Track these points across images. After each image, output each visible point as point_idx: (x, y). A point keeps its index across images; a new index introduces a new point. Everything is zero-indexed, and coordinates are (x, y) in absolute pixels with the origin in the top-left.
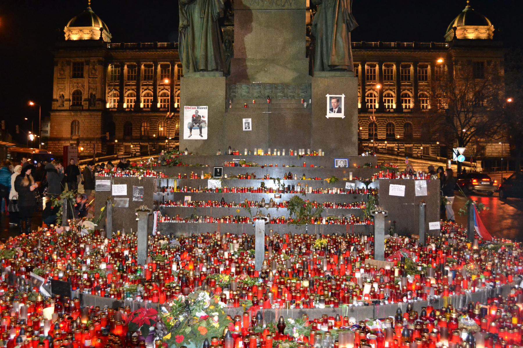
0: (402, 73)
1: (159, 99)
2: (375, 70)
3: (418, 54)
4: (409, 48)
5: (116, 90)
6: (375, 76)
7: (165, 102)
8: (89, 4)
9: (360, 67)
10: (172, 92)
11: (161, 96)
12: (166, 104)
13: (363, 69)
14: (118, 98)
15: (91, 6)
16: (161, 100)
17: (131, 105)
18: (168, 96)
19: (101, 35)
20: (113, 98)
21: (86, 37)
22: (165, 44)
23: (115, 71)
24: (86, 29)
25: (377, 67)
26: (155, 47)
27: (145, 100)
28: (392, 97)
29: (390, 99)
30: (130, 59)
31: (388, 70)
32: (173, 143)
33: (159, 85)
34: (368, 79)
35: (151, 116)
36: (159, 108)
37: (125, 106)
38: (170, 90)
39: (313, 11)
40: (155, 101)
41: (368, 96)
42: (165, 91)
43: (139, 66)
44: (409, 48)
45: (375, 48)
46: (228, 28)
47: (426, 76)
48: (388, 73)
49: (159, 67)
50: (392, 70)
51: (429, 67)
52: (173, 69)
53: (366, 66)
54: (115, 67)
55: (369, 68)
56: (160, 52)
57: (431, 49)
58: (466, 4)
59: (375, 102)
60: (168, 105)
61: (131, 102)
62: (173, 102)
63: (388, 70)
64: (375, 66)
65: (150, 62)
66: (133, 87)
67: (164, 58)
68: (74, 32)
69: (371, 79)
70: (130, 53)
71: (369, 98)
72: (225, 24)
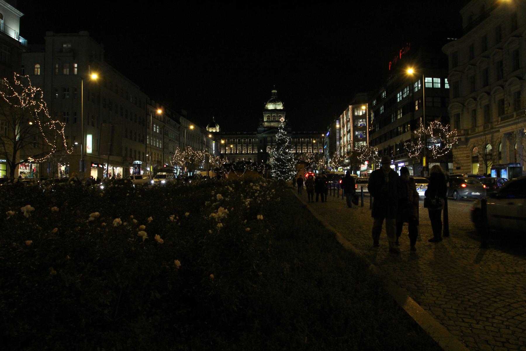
5: (223, 147)
6: (305, 142)
9: (301, 140)
11: (238, 149)
13: (302, 140)
18: (240, 149)
20: (223, 150)
21: (214, 131)
22: (239, 133)
24: (214, 129)
40: (237, 151)
46: (260, 129)
47: (322, 142)
49: (237, 140)
62: (242, 151)
68: (210, 129)
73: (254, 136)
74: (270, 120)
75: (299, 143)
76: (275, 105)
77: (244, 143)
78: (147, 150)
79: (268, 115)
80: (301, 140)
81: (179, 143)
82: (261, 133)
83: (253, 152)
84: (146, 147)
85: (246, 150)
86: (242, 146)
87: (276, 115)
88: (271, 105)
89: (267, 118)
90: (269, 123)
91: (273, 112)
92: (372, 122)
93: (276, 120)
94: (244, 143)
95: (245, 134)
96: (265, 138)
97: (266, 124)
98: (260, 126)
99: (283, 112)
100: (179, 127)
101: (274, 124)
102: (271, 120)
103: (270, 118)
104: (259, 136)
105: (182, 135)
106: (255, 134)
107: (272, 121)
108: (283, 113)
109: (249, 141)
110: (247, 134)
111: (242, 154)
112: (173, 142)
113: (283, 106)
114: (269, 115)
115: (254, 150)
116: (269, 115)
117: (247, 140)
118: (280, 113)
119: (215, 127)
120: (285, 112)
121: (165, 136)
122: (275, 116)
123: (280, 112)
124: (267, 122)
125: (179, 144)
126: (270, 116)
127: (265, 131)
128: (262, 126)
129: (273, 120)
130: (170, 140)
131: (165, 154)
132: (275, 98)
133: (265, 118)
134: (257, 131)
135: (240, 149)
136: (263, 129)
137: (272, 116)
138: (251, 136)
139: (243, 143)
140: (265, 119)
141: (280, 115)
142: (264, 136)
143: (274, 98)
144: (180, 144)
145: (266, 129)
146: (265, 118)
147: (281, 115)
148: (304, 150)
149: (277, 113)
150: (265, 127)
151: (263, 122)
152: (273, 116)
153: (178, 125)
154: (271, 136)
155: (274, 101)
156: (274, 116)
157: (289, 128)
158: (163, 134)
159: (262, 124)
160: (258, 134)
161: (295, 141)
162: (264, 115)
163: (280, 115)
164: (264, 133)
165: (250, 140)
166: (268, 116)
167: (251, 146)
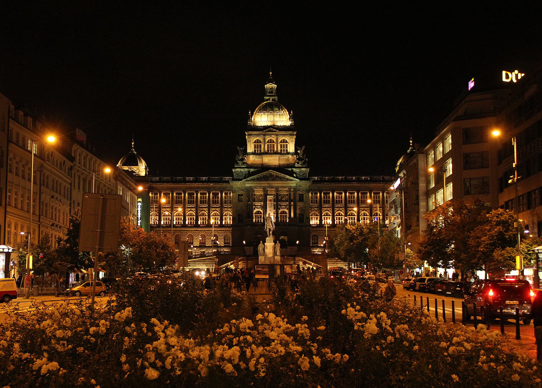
0: (362, 198)
1: (187, 218)
2: (342, 196)
3: (372, 185)
4: (366, 181)
6: (342, 201)
7: (191, 220)
8: (133, 146)
10: (196, 213)
11: (189, 216)
12: (192, 221)
14: (157, 217)
15: (134, 148)
16: (188, 218)
17: (166, 222)
18: (193, 216)
19: (146, 173)
23: (155, 197)
25: (343, 194)
26: (185, 181)
27: (176, 218)
28: (354, 215)
29: (353, 217)
30: (166, 189)
31: (351, 196)
32: (198, 250)
33: (187, 208)
34: (337, 203)
35: (182, 230)
36: (188, 225)
37: (162, 223)
38: (195, 211)
39: (296, 156)
40: (185, 220)
41: (337, 215)
42: (191, 212)
43: (173, 194)
44: (366, 181)
45: (342, 181)
46: (237, 169)
48: (352, 198)
49: (187, 194)
50: (354, 196)
51: (381, 194)
52: (197, 197)
53: (335, 194)
54: (155, 195)
55: (338, 195)
56: (188, 185)
57: (380, 181)
58: (410, 146)
59: (342, 220)
60: (193, 222)
61: (166, 220)
62: (197, 220)
63: (351, 196)
64: (342, 193)
65: (180, 191)
66: (168, 209)
67: (191, 188)
69: (339, 203)
70: (165, 185)
71: (338, 217)
72: (235, 167)
73: (225, 185)
74: (260, 150)
75: (327, 202)
76: (272, 116)
77: (202, 202)
78: (7, 219)
79: (258, 140)
80: (331, 194)
81: (70, 203)
82: (241, 180)
83: (221, 222)
84: (6, 212)
85: (207, 217)
86: (197, 208)
87: (275, 141)
88: (263, 116)
89: (255, 145)
90: (258, 156)
91: (268, 131)
92: (514, 164)
93: (273, 150)
94: (201, 201)
95: (203, 182)
96: (250, 192)
97: (252, 159)
98: (238, 163)
99: (290, 132)
100: (71, 168)
101: (270, 158)
102: (262, 151)
103: (261, 145)
104: (237, 184)
105: (76, 185)
106: (228, 182)
107: (266, 153)
108: (291, 135)
109: (213, 198)
110: (208, 181)
111: (197, 225)
112: (57, 202)
113: (290, 119)
114: (258, 138)
115: (224, 217)
116: (258, 138)
117: (209, 194)
118: (284, 135)
119: (137, 165)
120: (295, 133)
121: (42, 187)
122: (274, 142)
123: (283, 132)
124: (254, 153)
125: (70, 206)
126: (260, 142)
127: (250, 174)
128: (244, 163)
129: (268, 150)
130: (52, 197)
131: (41, 229)
132: (273, 100)
133: (251, 147)
134: (231, 174)
135: (193, 216)
136: (246, 170)
137: (267, 141)
138: (218, 185)
139: (199, 203)
140: (250, 148)
141: (284, 138)
142: (248, 185)
143: (271, 101)
144: (72, 205)
145: (252, 170)
146: (251, 147)
147: (288, 141)
148: (339, 219)
149: (277, 135)
150: (249, 166)
151: (245, 153)
152: (268, 142)
153: (69, 164)
154: (264, 185)
155: (270, 108)
156: (271, 141)
157: (303, 169)
158: (38, 183)
159: (242, 160)
160: (235, 182)
161: (317, 197)
162: (247, 141)
163: (284, 140)
164: (248, 179)
165: (215, 195)
166: (258, 141)
167: (217, 209)
